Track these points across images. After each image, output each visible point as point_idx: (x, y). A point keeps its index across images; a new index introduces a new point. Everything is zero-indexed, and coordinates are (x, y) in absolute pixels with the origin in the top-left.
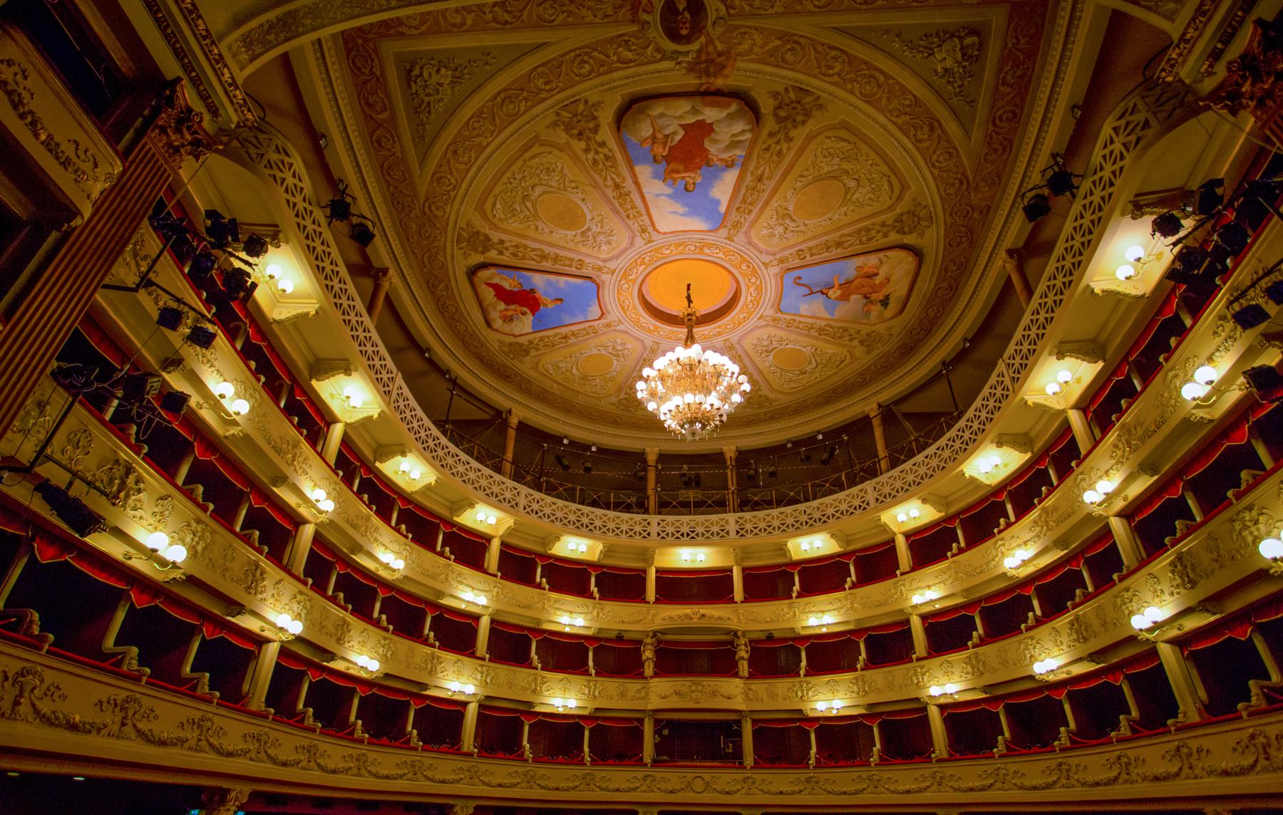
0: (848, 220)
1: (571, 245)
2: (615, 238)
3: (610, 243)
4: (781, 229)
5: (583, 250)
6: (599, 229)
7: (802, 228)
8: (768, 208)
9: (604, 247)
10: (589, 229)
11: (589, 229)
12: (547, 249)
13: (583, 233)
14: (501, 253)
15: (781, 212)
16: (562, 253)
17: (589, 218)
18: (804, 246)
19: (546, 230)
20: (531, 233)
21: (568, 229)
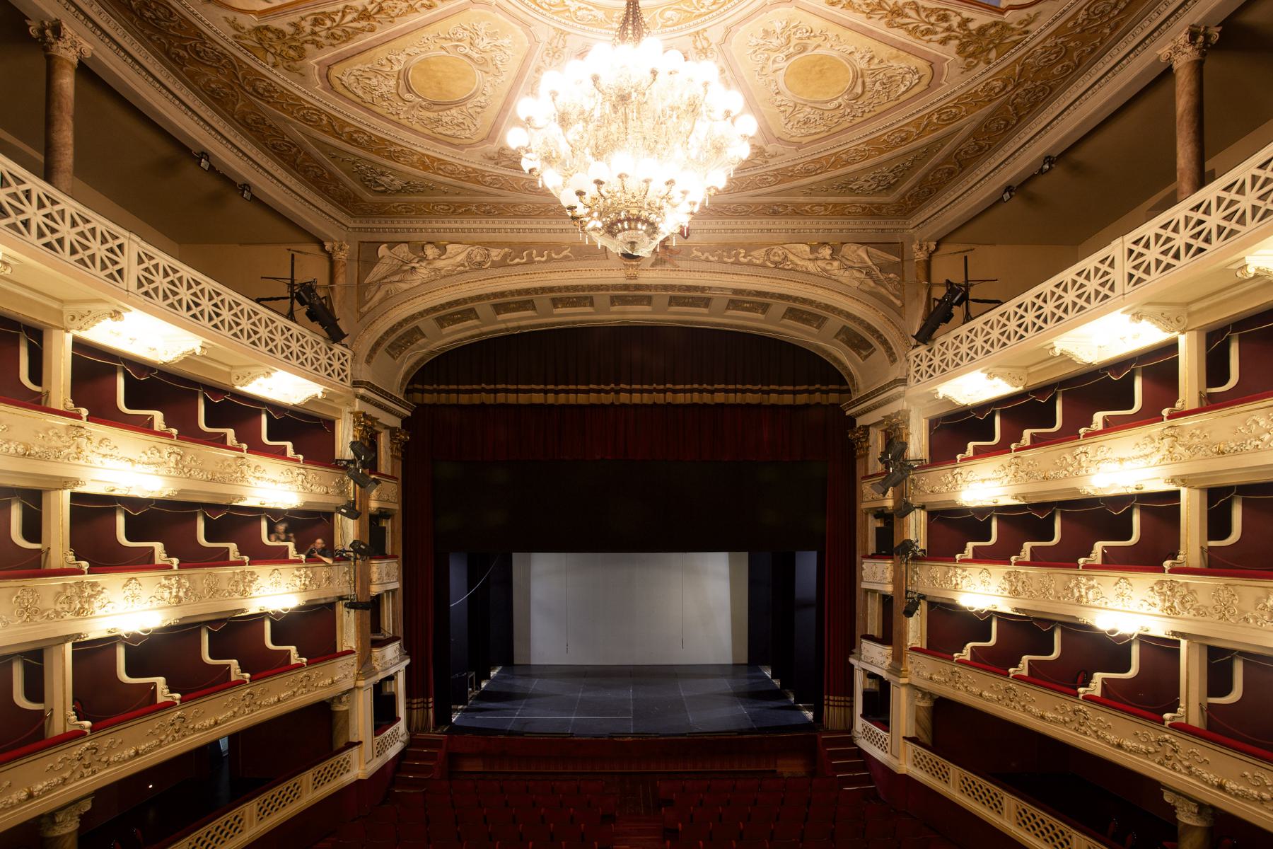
0: (381, 53)
1: (833, 30)
2: (754, 41)
3: (766, 32)
4: (483, 44)
5: (817, 24)
6: (773, 55)
7: (447, 44)
8: (514, 74)
9: (778, 26)
10: (788, 57)
11: (788, 57)
12: (878, 25)
13: (804, 49)
14: (965, 22)
15: (491, 68)
16: (859, 19)
17: (782, 72)
18: (426, 15)
19: (857, 56)
20: (884, 51)
21: (823, 57)
